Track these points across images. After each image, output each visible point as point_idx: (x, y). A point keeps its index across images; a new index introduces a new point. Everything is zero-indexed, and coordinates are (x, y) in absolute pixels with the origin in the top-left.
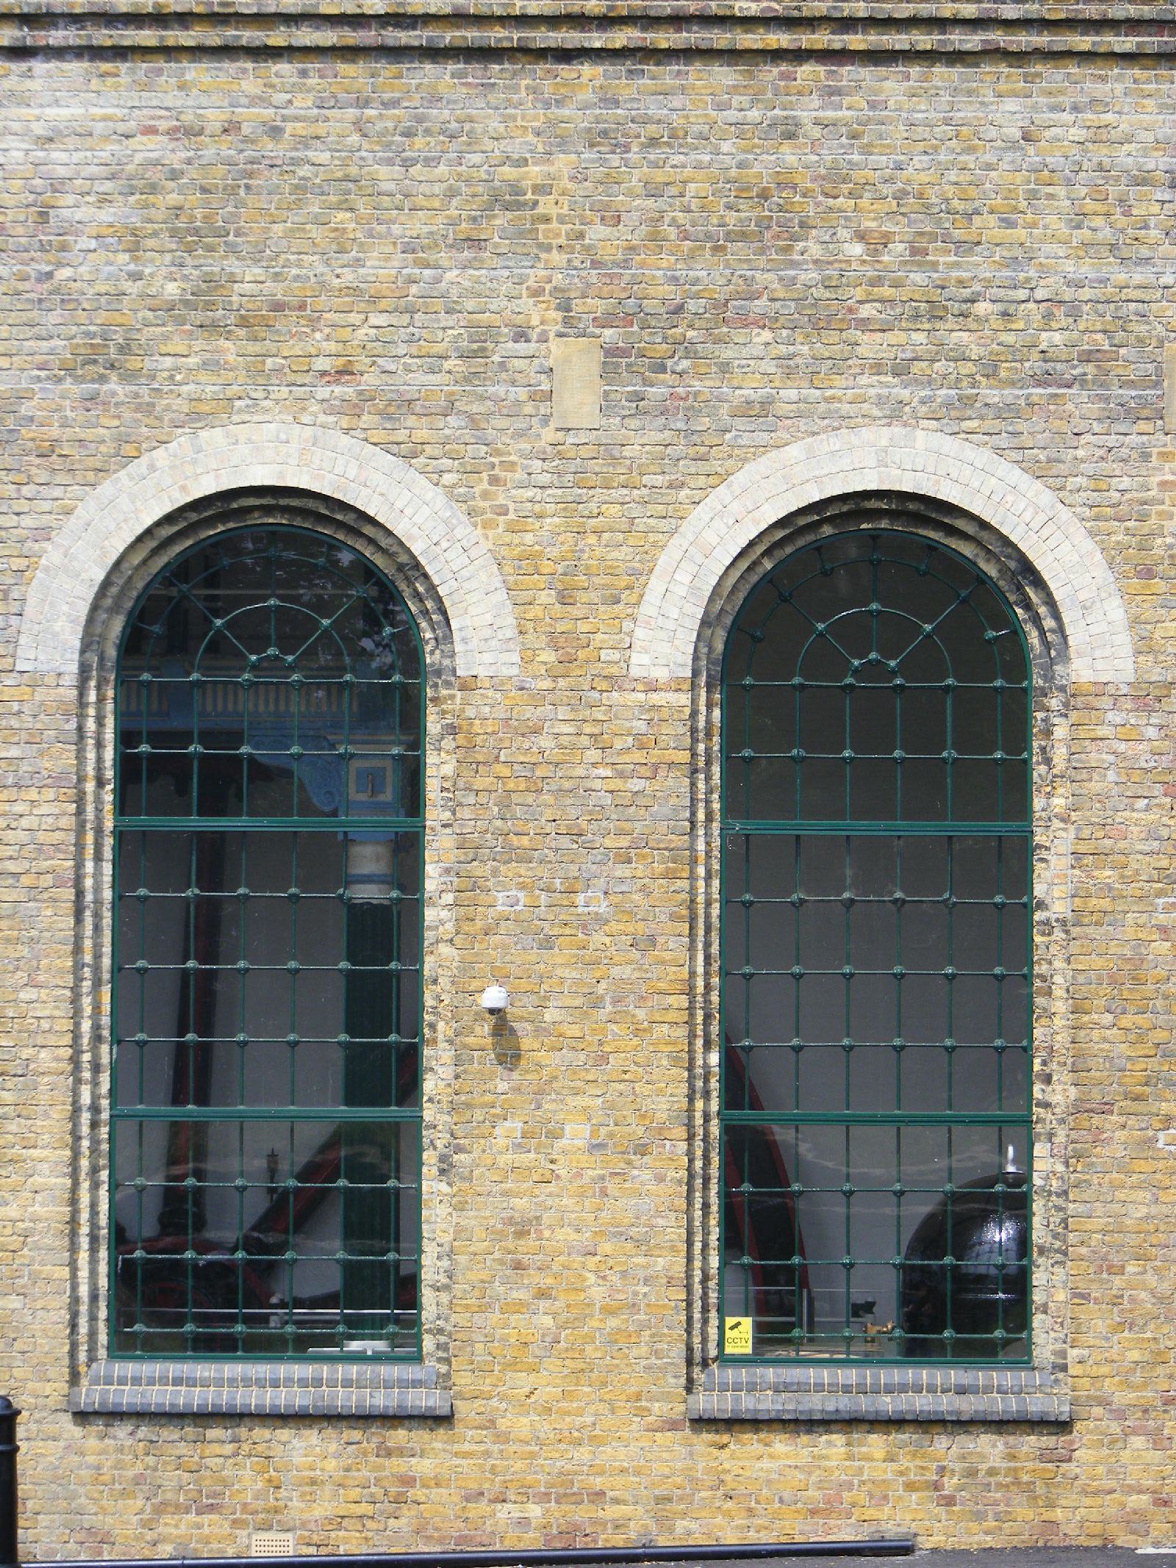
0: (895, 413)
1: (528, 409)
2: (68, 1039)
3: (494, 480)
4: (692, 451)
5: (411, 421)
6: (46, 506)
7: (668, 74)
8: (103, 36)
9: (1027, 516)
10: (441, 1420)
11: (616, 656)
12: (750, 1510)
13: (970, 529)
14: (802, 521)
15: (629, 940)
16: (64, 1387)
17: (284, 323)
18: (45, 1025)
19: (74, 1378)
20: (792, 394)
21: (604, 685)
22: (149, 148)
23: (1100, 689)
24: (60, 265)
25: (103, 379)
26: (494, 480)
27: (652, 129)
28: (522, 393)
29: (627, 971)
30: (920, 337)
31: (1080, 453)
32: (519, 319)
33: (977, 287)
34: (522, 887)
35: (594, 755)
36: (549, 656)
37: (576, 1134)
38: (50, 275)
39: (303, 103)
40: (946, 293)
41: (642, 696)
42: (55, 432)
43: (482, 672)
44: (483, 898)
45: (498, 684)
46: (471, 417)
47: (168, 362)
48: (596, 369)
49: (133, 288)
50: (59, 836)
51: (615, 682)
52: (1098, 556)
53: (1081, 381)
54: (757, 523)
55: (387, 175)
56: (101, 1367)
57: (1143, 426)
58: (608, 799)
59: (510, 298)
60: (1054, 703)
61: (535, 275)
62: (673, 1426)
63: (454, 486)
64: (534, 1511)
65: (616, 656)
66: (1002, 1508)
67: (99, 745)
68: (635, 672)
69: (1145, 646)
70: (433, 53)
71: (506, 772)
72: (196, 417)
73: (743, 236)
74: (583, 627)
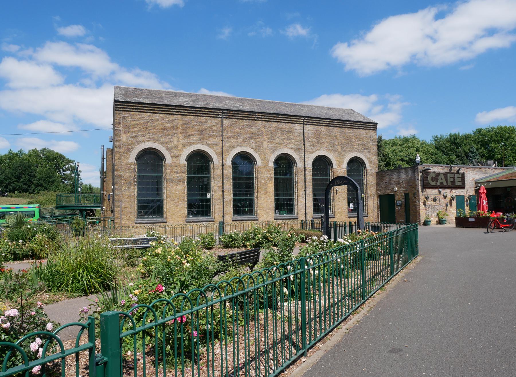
0: (356, 151)
8: (312, 123)
22: (314, 131)
37: (341, 198)
39: (323, 129)
51: (342, 168)
55: (328, 134)
69: (370, 167)
72: (318, 150)
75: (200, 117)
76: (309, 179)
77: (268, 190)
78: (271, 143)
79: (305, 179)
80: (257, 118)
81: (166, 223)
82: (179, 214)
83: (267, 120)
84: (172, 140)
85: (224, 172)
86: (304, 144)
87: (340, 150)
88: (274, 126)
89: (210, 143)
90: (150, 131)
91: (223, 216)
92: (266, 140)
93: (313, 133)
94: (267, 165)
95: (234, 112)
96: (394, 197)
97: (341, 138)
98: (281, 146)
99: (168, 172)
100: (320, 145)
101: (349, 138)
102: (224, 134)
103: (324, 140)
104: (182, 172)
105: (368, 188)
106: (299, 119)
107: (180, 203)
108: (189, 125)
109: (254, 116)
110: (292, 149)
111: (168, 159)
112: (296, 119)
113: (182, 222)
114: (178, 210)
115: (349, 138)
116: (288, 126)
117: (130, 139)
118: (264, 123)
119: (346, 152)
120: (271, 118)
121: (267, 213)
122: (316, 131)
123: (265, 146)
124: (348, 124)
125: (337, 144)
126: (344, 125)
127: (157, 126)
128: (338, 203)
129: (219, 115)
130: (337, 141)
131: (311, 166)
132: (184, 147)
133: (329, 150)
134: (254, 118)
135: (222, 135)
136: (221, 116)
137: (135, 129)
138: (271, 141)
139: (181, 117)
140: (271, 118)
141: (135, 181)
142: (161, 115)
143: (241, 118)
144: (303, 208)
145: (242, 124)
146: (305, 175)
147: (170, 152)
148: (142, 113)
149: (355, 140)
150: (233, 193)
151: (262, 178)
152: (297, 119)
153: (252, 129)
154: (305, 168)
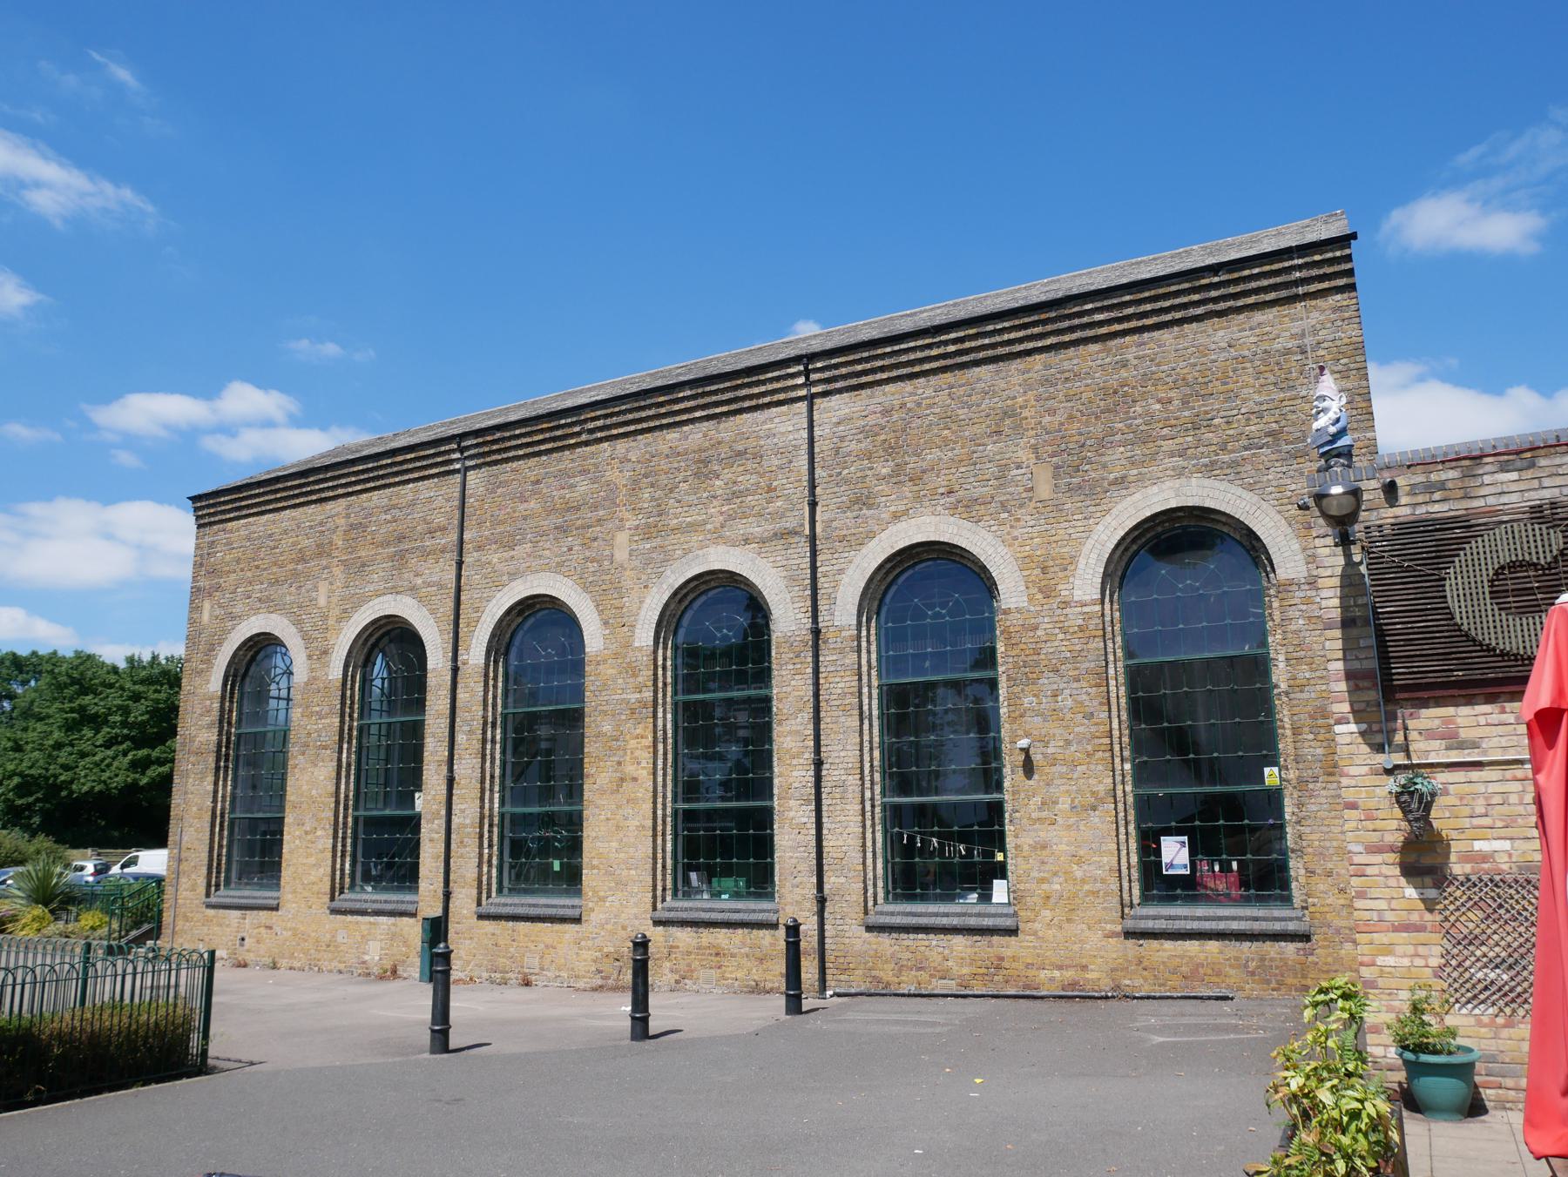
0: (1180, 473)
1: (1024, 495)
2: (859, 771)
3: (1011, 527)
4: (1093, 503)
5: (977, 507)
6: (843, 560)
7: (1071, 351)
8: (854, 381)
9: (1247, 509)
10: (1012, 932)
11: (1067, 593)
12: (1155, 976)
13: (1224, 519)
14: (1146, 526)
15: (1082, 715)
16: (862, 915)
18: (850, 765)
19: (866, 912)
20: (1135, 472)
21: (1063, 606)
22: (871, 420)
23: (1291, 582)
24: (844, 469)
25: (861, 509)
26: (1011, 527)
27: (1067, 375)
28: (1021, 489)
29: (1081, 729)
30: (1190, 439)
31: (1270, 477)
32: (1019, 460)
33: (1215, 413)
34: (1035, 696)
35: (1061, 636)
36: (1039, 596)
37: (1064, 804)
38: (840, 473)
39: (929, 392)
40: (1200, 418)
41: (1080, 609)
42: (845, 532)
43: (1012, 606)
44: (1018, 702)
45: (1018, 610)
46: (1001, 502)
47: (884, 499)
48: (1050, 475)
49: (869, 473)
50: (852, 689)
51: (1066, 604)
52: (1283, 521)
53: (1267, 445)
54: (1123, 529)
55: (962, 413)
56: (878, 908)
57: (1299, 460)
58: (1068, 655)
59: (1013, 452)
60: (1272, 592)
61: (1022, 442)
62: (1113, 935)
63: (996, 531)
64: (1057, 974)
65: (1067, 593)
66: (1279, 978)
67: (869, 652)
68: (1076, 599)
70: (977, 363)
71: (1024, 647)
72: (896, 517)
73: (1109, 411)
74: (1053, 582)
75: (396, 489)
76: (843, 695)
77: (630, 769)
78: (647, 532)
79: (817, 695)
80: (591, 431)
83: (632, 428)
86: (813, 505)
87: (1044, 490)
88: (665, 449)
89: (419, 581)
91: (447, 896)
92: (628, 525)
94: (628, 645)
95: (498, 435)
97: (1052, 412)
98: (695, 538)
100: (907, 490)
101: (1117, 399)
103: (931, 456)
106: (778, 379)
107: (319, 833)
109: (577, 429)
110: (747, 541)
112: (763, 382)
115: (1117, 399)
116: (728, 429)
118: (621, 446)
120: (643, 414)
121: (621, 884)
122: (887, 412)
123: (621, 555)
124: (1098, 317)
125: (1024, 455)
126: (1072, 329)
128: (1045, 834)
129: (451, 462)
130: (1029, 439)
133: (967, 508)
134: (578, 434)
135: (461, 541)
137: (233, 576)
138: (648, 526)
139: (343, 502)
140: (643, 414)
143: (530, 450)
144: (803, 867)
145: (532, 476)
146: (816, 672)
147: (306, 638)
148: (251, 519)
151: (605, 713)
152: (772, 380)
153: (572, 486)
154: (816, 632)
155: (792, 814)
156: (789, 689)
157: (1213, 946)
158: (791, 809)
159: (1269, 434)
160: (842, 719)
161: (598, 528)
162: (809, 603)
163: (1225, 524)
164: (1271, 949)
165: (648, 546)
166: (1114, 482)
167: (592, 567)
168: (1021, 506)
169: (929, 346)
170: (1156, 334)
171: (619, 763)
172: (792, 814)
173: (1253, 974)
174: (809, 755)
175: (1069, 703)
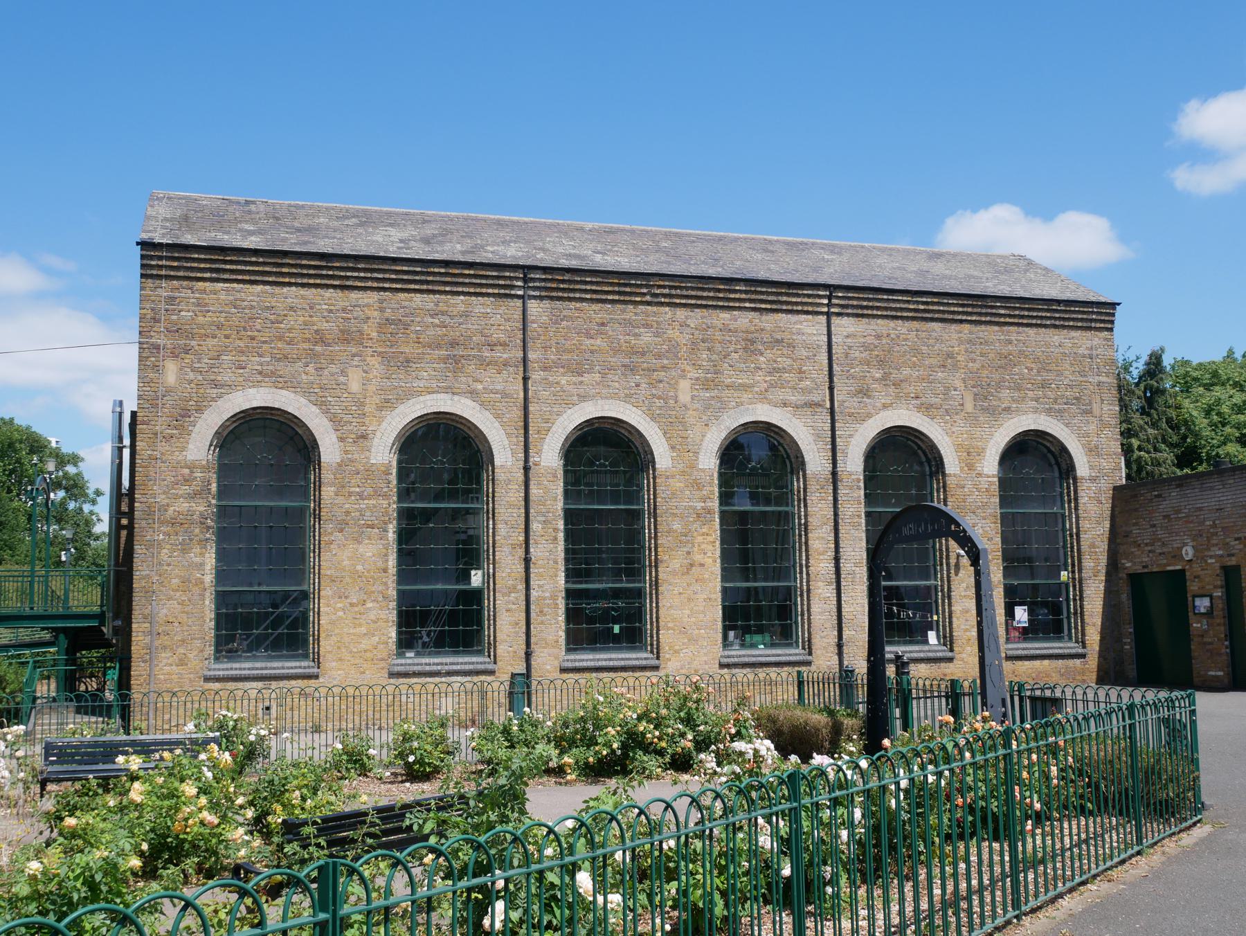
0: (1036, 411)
7: (983, 327)
8: (860, 311)
17: (903, 385)
22: (870, 340)
36: (966, 468)
39: (904, 331)
45: (955, 475)
51: (980, 475)
69: (1091, 468)
70: (932, 320)
72: (885, 407)
75: (443, 297)
76: (852, 517)
77: (698, 557)
78: (706, 384)
79: (836, 515)
81: (316, 677)
82: (365, 644)
83: (693, 302)
84: (342, 379)
85: (534, 491)
86: (831, 389)
87: (969, 407)
88: (719, 324)
89: (480, 387)
90: (265, 346)
91: (528, 655)
92: (689, 375)
93: (866, 347)
96: (1185, 581)
97: (974, 361)
98: (746, 396)
99: (328, 492)
100: (892, 390)
102: (532, 356)
103: (906, 372)
104: (377, 494)
105: (1084, 548)
106: (809, 296)
107: (369, 605)
108: (407, 326)
109: (645, 291)
110: (785, 405)
111: (330, 449)
112: (798, 295)
113: (376, 675)
114: (363, 630)
115: (1007, 362)
116: (770, 322)
117: (191, 376)
118: (681, 313)
119: (996, 414)
120: (705, 294)
121: (693, 640)
122: (878, 337)
123: (685, 397)
125: (958, 384)
126: (986, 314)
127: (290, 330)
129: (512, 287)
130: (960, 374)
131: (860, 468)
132: (387, 404)
133: (927, 409)
134: (644, 294)
135: (525, 360)
136: (520, 293)
137: (211, 342)
138: (707, 380)
140: (705, 294)
141: (208, 528)
142: (302, 291)
143: (594, 296)
144: (828, 625)
145: (598, 318)
147: (336, 422)
148: (235, 285)
149: (1030, 369)
150: (567, 570)
151: (675, 515)
152: (805, 295)
153: (636, 335)
154: (834, 474)
155: (820, 591)
156: (817, 509)
157: (1046, 662)
158: (819, 588)
159: (1076, 398)
160: (853, 531)
161: (663, 373)
162: (830, 454)
163: (1051, 442)
164: (1071, 662)
165: (708, 395)
166: (1004, 410)
167: (659, 403)
168: (957, 414)
169: (908, 302)
170: (1026, 329)
171: (688, 553)
172: (820, 591)
173: (1063, 675)
174: (831, 554)
175: (981, 531)
